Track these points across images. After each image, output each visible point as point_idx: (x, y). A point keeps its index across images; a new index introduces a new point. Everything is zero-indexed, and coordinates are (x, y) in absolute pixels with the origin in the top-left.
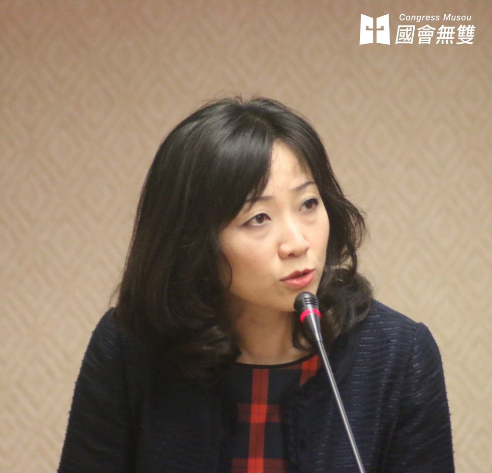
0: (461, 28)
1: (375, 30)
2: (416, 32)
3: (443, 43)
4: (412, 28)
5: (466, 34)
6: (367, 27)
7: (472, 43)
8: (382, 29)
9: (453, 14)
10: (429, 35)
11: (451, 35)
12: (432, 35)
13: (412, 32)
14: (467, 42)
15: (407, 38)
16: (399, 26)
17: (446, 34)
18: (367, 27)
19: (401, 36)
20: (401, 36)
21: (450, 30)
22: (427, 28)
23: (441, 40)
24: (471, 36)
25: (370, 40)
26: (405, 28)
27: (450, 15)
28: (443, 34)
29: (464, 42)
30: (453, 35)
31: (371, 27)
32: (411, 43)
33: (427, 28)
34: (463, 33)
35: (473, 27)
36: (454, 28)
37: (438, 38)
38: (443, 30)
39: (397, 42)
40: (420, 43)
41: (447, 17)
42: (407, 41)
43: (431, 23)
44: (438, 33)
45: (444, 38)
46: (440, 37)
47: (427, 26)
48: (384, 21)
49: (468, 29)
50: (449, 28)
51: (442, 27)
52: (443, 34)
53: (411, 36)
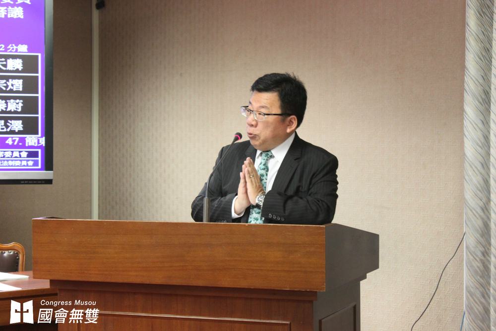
0: (88, 311)
1: (22, 312)
2: (54, 314)
3: (74, 322)
4: (51, 311)
5: (92, 316)
6: (16, 310)
7: (96, 323)
8: (27, 311)
9: (82, 300)
10: (63, 316)
11: (81, 316)
12: (66, 317)
13: (50, 314)
14: (93, 322)
15: (47, 319)
16: (41, 310)
17: (76, 315)
18: (16, 310)
19: (42, 317)
20: (42, 317)
21: (80, 313)
22: (62, 311)
23: (73, 320)
24: (96, 317)
25: (20, 322)
26: (45, 311)
27: (79, 301)
28: (74, 316)
29: (90, 322)
30: (82, 316)
31: (19, 310)
32: (50, 322)
33: (62, 311)
34: (90, 315)
35: (97, 310)
36: (83, 310)
37: (70, 318)
38: (75, 312)
39: (39, 322)
40: (56, 322)
41: (77, 303)
42: (46, 321)
43: (65, 307)
44: (70, 315)
45: (75, 318)
46: (72, 318)
47: (62, 309)
48: (29, 305)
49: (93, 311)
50: (79, 311)
51: (74, 310)
52: (74, 316)
53: (49, 317)
